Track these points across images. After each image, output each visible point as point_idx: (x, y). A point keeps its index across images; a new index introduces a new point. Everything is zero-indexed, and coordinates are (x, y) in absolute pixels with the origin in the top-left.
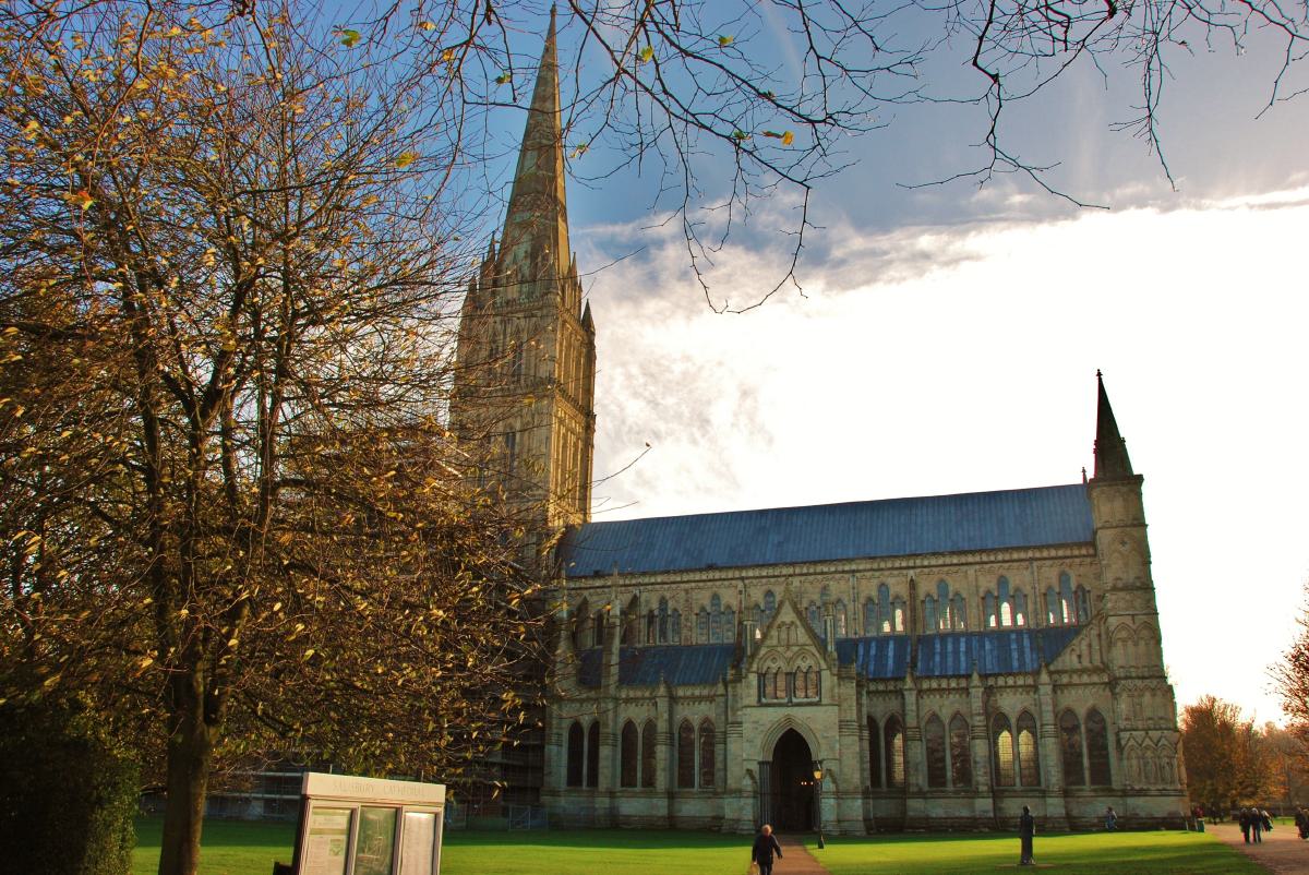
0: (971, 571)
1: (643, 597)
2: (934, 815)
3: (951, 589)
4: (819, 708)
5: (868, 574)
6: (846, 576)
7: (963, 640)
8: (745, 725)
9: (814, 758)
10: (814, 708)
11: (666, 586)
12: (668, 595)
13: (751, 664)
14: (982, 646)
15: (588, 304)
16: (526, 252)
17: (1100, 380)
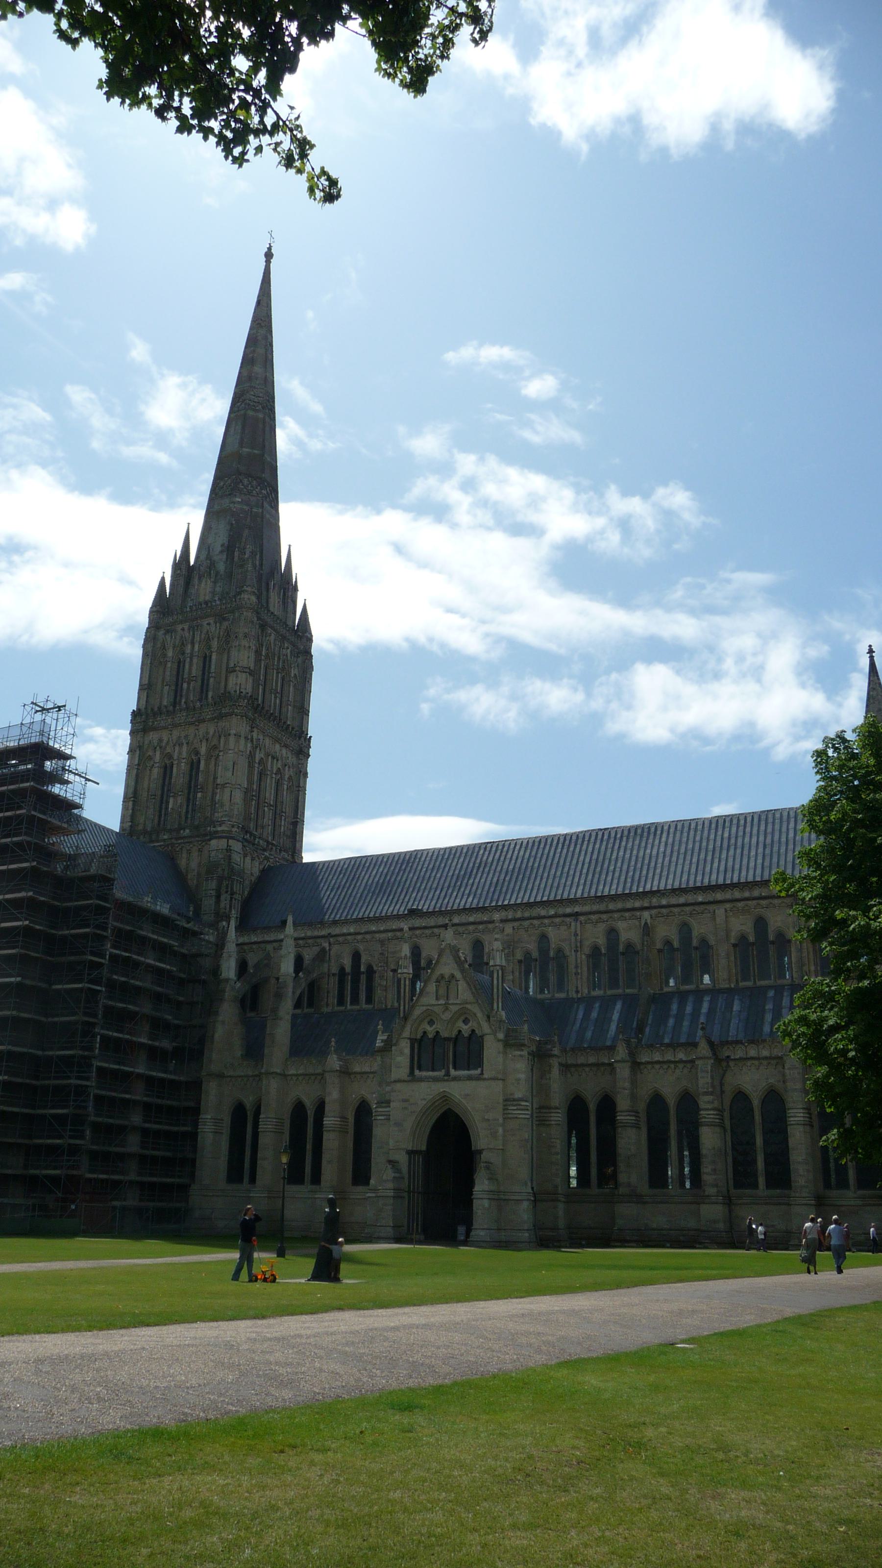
0: (720, 911)
1: (335, 949)
2: (655, 1226)
3: (695, 933)
4: (481, 1083)
5: (594, 917)
6: (568, 920)
7: (707, 999)
8: (392, 1104)
9: (473, 1148)
10: (474, 1083)
11: (359, 937)
12: (361, 947)
13: (403, 1027)
14: (730, 1006)
15: (305, 606)
16: (222, 545)
17: (872, 658)
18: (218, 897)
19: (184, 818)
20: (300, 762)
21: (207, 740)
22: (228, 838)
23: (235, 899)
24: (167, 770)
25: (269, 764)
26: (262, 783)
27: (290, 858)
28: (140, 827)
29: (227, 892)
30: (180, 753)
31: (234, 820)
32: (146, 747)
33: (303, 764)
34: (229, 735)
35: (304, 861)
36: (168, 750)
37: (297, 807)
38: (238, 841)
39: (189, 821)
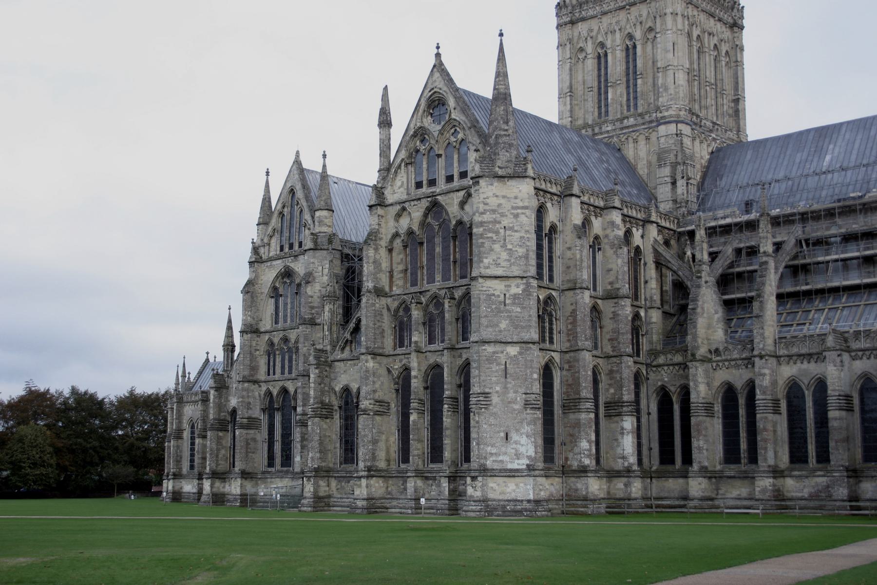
18: (674, 183)
19: (625, 108)
20: (736, 35)
21: (641, 23)
22: (677, 122)
23: (691, 184)
24: (601, 59)
25: (706, 40)
26: (701, 63)
27: (735, 137)
28: (580, 122)
29: (683, 177)
30: (613, 41)
31: (681, 103)
32: (575, 40)
33: (738, 37)
34: (665, 14)
35: (750, 139)
36: (600, 39)
37: (737, 83)
38: (687, 124)
39: (632, 110)
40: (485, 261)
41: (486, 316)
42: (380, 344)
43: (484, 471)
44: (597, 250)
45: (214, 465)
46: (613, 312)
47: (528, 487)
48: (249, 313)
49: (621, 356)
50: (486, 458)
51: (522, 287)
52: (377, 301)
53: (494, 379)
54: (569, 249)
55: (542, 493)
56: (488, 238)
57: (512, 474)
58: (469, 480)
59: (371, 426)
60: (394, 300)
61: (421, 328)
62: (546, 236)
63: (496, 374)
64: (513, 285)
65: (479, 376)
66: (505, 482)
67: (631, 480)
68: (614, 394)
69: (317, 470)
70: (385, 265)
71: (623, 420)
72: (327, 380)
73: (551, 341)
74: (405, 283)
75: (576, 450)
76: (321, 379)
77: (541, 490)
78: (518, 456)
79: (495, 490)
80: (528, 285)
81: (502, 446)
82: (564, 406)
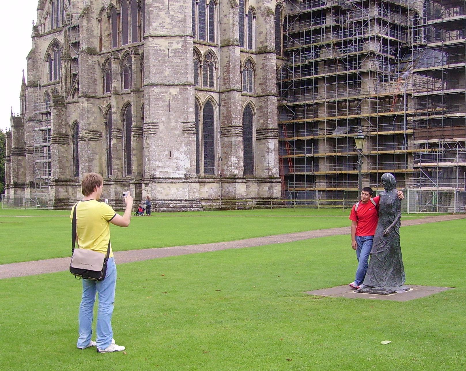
40: (154, 24)
41: (154, 66)
42: (93, 90)
43: (153, 179)
44: (252, 18)
45: (15, 179)
46: (263, 64)
47: (185, 190)
48: (32, 73)
49: (268, 96)
50: (155, 170)
51: (181, 43)
52: (90, 58)
53: (161, 112)
54: (226, 16)
55: (196, 195)
56: (156, 7)
57: (174, 181)
58: (143, 185)
59: (87, 149)
60: (102, 57)
61: (119, 77)
62: (207, 6)
63: (162, 109)
64: (174, 42)
65: (149, 110)
66: (168, 187)
67: (273, 184)
68: (263, 124)
69: (57, 181)
70: (96, 32)
71: (268, 142)
72: (63, 118)
73: (212, 85)
74: (110, 44)
75: (229, 163)
76: (59, 116)
77: (195, 192)
78: (178, 168)
79: (162, 193)
80: (186, 42)
81: (167, 161)
82: (221, 132)
